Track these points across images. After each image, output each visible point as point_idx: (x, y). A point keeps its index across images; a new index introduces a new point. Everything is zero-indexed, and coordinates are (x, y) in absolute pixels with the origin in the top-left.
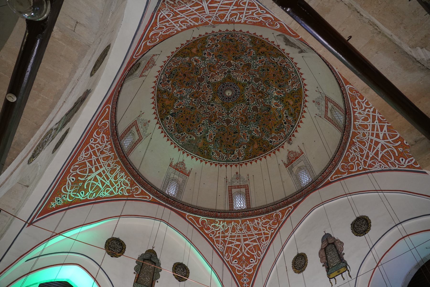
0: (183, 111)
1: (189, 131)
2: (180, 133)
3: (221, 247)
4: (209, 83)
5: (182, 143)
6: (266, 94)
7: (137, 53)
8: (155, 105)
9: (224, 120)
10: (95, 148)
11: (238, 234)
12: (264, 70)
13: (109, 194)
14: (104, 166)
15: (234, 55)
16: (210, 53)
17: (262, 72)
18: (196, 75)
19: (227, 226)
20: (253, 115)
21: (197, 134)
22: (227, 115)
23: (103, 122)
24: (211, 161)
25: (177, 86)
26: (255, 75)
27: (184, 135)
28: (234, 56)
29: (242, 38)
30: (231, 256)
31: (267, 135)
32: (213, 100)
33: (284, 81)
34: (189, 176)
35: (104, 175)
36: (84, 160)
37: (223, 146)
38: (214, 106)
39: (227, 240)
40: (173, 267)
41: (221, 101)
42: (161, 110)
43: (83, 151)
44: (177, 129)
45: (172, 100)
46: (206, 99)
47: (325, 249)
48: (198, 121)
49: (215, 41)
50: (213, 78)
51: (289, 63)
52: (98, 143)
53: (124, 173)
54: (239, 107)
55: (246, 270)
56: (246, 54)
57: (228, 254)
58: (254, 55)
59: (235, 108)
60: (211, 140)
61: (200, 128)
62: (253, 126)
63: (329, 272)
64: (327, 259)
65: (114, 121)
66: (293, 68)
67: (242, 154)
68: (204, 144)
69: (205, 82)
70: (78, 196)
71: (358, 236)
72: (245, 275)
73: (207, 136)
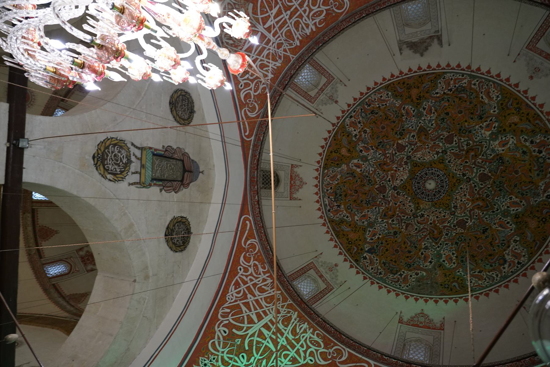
0: (384, 242)
1: (409, 266)
2: (396, 274)
4: (395, 188)
5: (407, 286)
6: (476, 145)
7: (245, 132)
8: (336, 241)
9: (454, 226)
10: (249, 282)
12: (443, 119)
13: (291, 363)
14: (271, 313)
15: (395, 131)
16: (366, 147)
17: (444, 124)
18: (371, 186)
20: (489, 188)
21: (426, 266)
22: (452, 216)
23: (249, 242)
25: (356, 210)
26: (441, 135)
27: (405, 275)
28: (396, 133)
29: (380, 100)
31: (535, 194)
32: (417, 208)
33: (476, 105)
34: (443, 330)
35: (273, 329)
36: (236, 301)
37: (480, 261)
38: (426, 216)
41: (430, 203)
42: (348, 248)
43: (232, 287)
44: (388, 269)
45: (358, 231)
46: (407, 211)
48: (416, 247)
49: (357, 126)
50: (397, 179)
51: (453, 75)
52: (251, 275)
53: (306, 323)
54: (461, 194)
56: (406, 118)
58: (414, 111)
59: (456, 198)
60: (454, 263)
61: (425, 256)
62: (503, 202)
65: (268, 247)
66: (465, 76)
67: (522, 252)
68: (445, 276)
69: (390, 190)
70: (237, 362)
73: (444, 261)
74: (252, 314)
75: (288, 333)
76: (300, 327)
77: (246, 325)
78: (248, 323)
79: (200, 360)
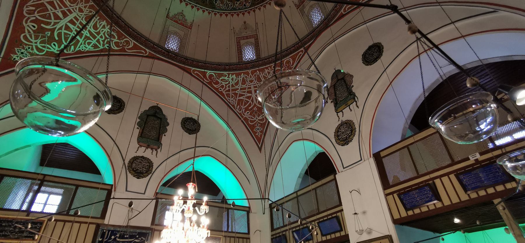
3: (232, 101)
11: (249, 85)
13: (93, 48)
19: (237, 79)
24: (215, 10)
30: (243, 108)
39: (237, 92)
40: (182, 122)
47: (334, 85)
55: (259, 120)
57: (240, 106)
63: (337, 107)
64: (335, 95)
71: (369, 65)
72: (257, 124)
74: (58, 12)
75: (90, 28)
76: (100, 24)
77: (53, 21)
78: (55, 19)
79: (16, 50)
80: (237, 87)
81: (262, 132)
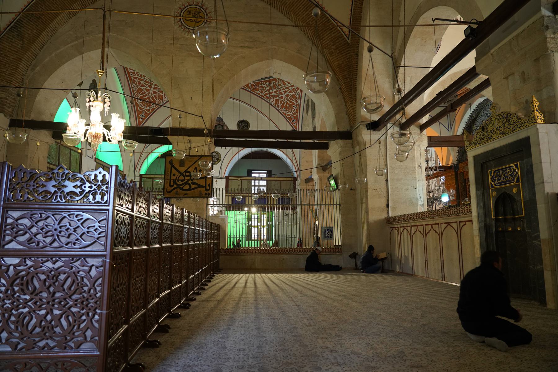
3: (135, 87)
55: (146, 109)
57: (138, 93)
80: (143, 78)
81: (144, 119)
